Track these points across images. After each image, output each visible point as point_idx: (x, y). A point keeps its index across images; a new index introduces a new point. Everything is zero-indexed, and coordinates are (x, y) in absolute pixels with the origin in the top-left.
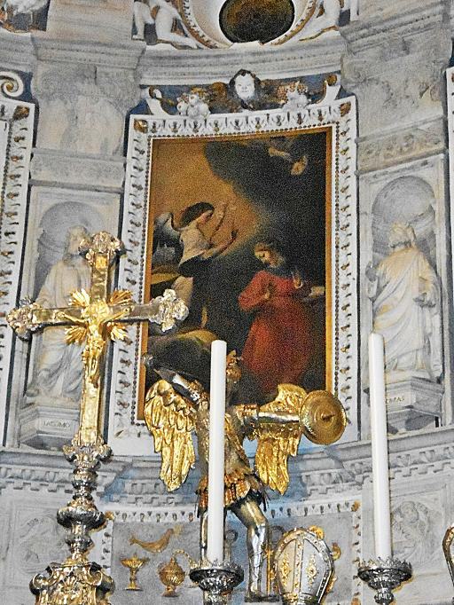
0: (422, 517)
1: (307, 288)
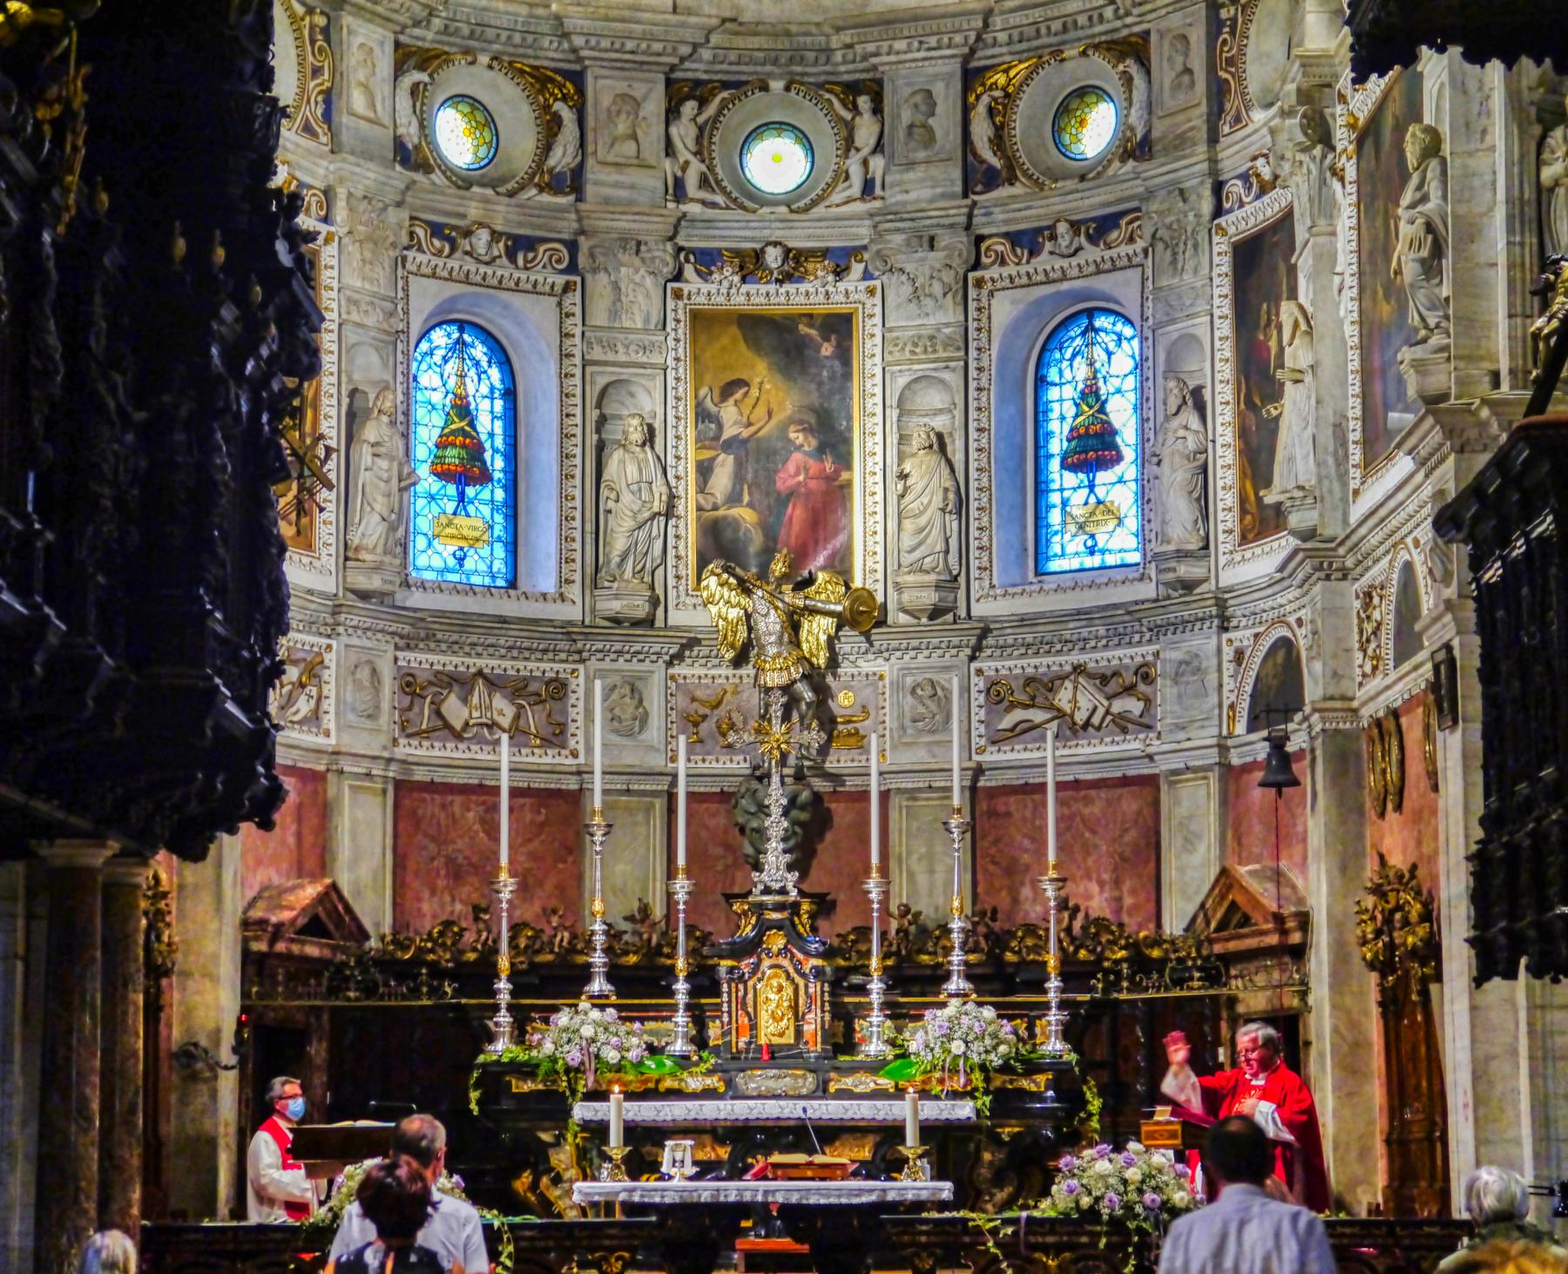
0: (940, 692)
1: (837, 473)
